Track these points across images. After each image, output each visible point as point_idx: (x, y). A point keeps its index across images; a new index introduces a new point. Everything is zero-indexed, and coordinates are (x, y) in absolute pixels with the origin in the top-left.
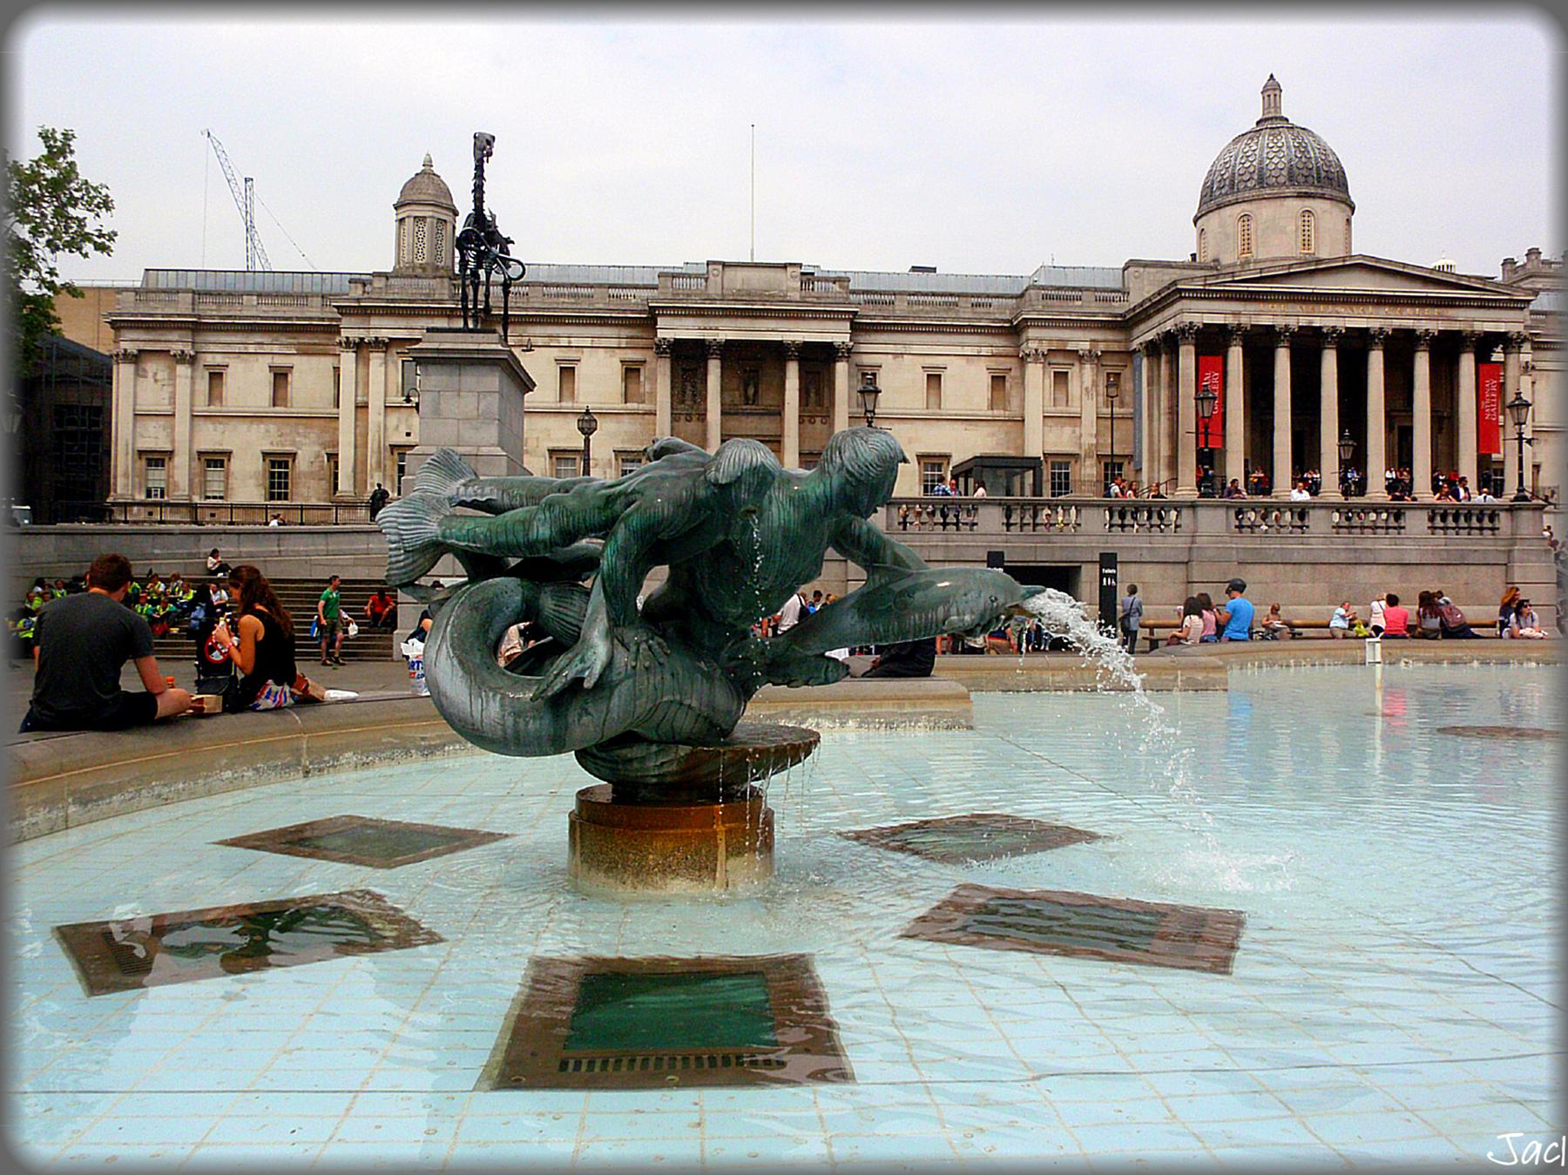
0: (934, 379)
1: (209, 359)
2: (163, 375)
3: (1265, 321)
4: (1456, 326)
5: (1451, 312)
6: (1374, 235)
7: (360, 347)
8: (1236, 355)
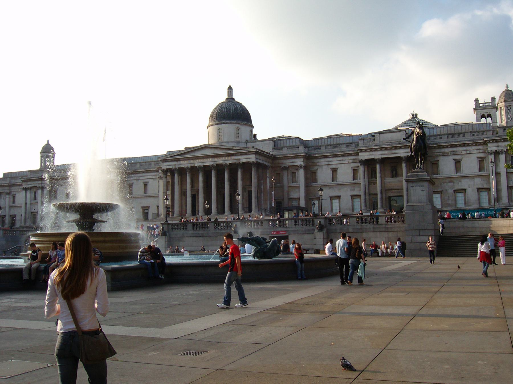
0: (146, 186)
1: (13, 193)
2: (5, 198)
3: (182, 166)
4: (235, 161)
5: (233, 158)
7: (26, 189)
8: (176, 176)
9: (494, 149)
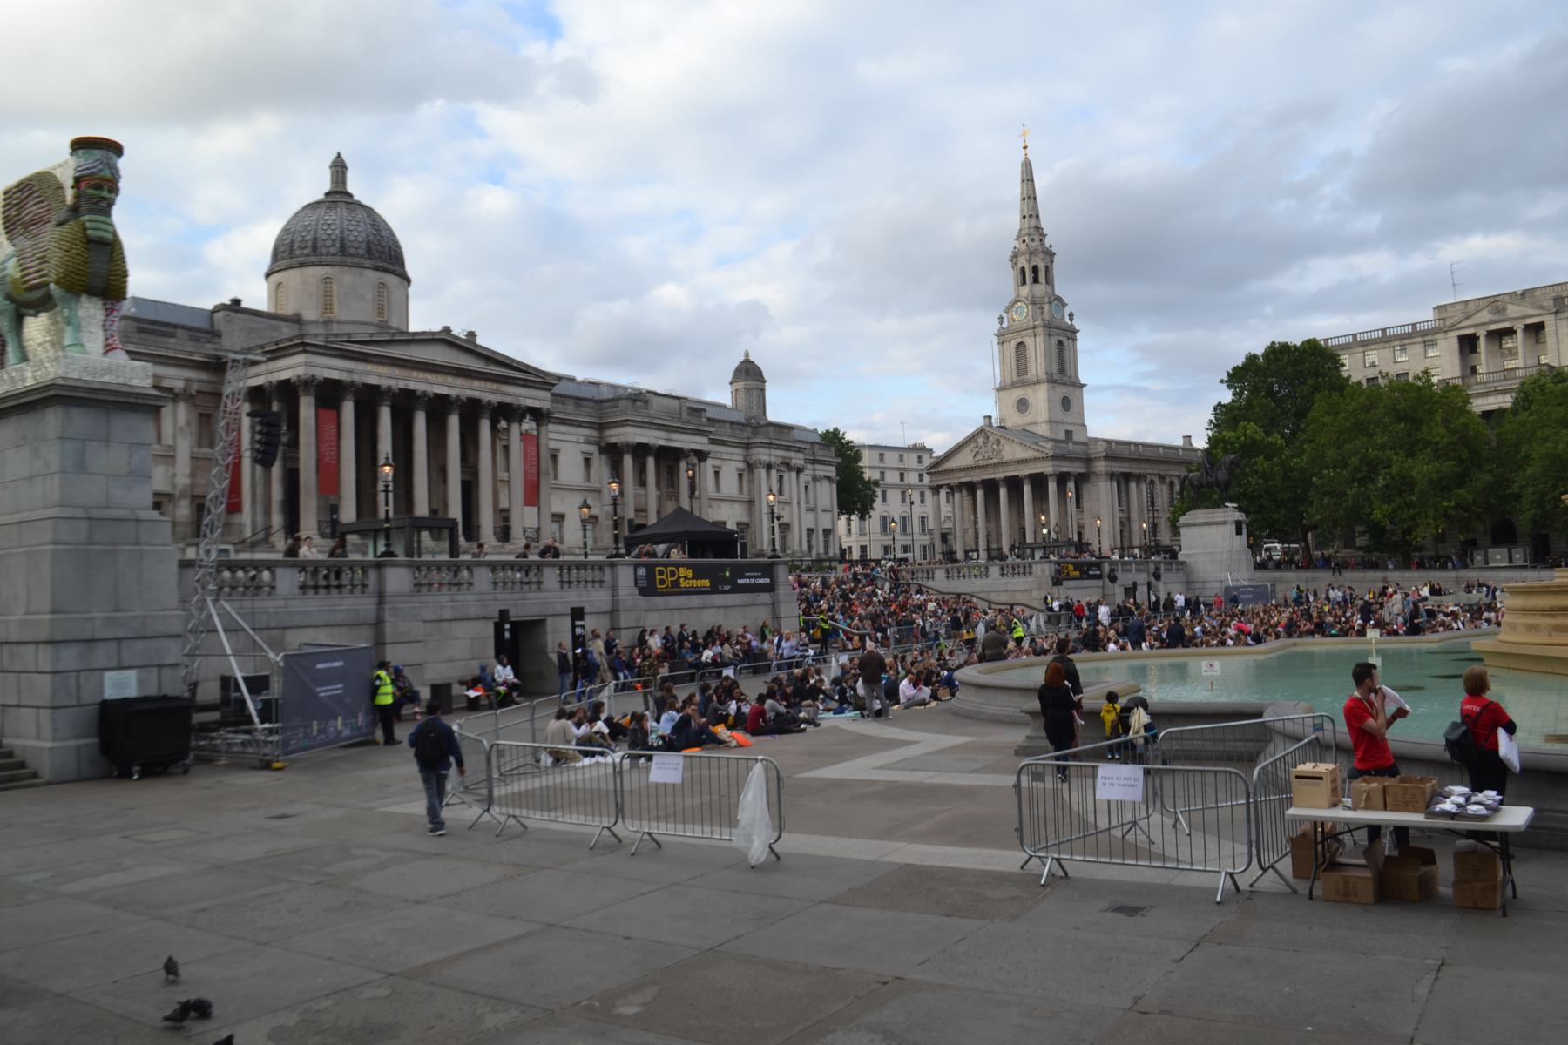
3: (373, 380)
4: (508, 400)
5: (505, 388)
6: (423, 315)
9: (765, 458)
